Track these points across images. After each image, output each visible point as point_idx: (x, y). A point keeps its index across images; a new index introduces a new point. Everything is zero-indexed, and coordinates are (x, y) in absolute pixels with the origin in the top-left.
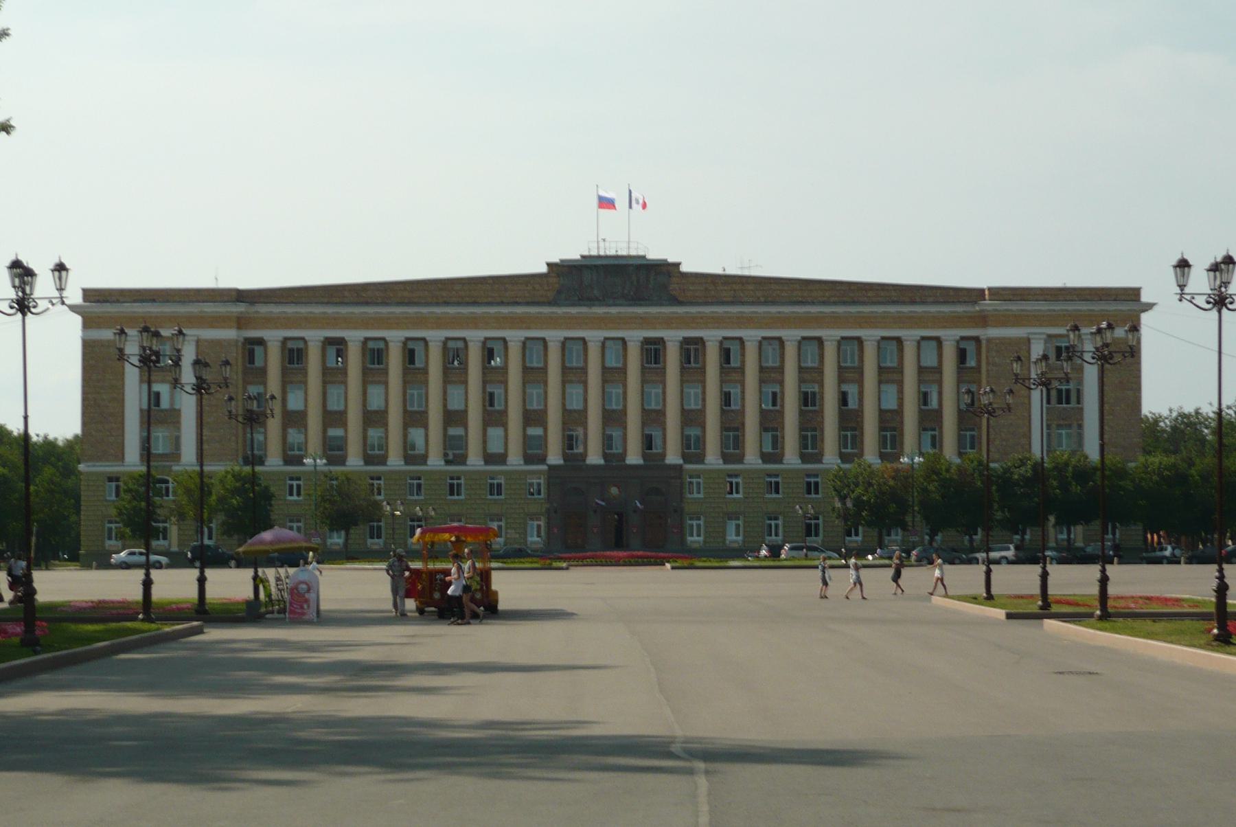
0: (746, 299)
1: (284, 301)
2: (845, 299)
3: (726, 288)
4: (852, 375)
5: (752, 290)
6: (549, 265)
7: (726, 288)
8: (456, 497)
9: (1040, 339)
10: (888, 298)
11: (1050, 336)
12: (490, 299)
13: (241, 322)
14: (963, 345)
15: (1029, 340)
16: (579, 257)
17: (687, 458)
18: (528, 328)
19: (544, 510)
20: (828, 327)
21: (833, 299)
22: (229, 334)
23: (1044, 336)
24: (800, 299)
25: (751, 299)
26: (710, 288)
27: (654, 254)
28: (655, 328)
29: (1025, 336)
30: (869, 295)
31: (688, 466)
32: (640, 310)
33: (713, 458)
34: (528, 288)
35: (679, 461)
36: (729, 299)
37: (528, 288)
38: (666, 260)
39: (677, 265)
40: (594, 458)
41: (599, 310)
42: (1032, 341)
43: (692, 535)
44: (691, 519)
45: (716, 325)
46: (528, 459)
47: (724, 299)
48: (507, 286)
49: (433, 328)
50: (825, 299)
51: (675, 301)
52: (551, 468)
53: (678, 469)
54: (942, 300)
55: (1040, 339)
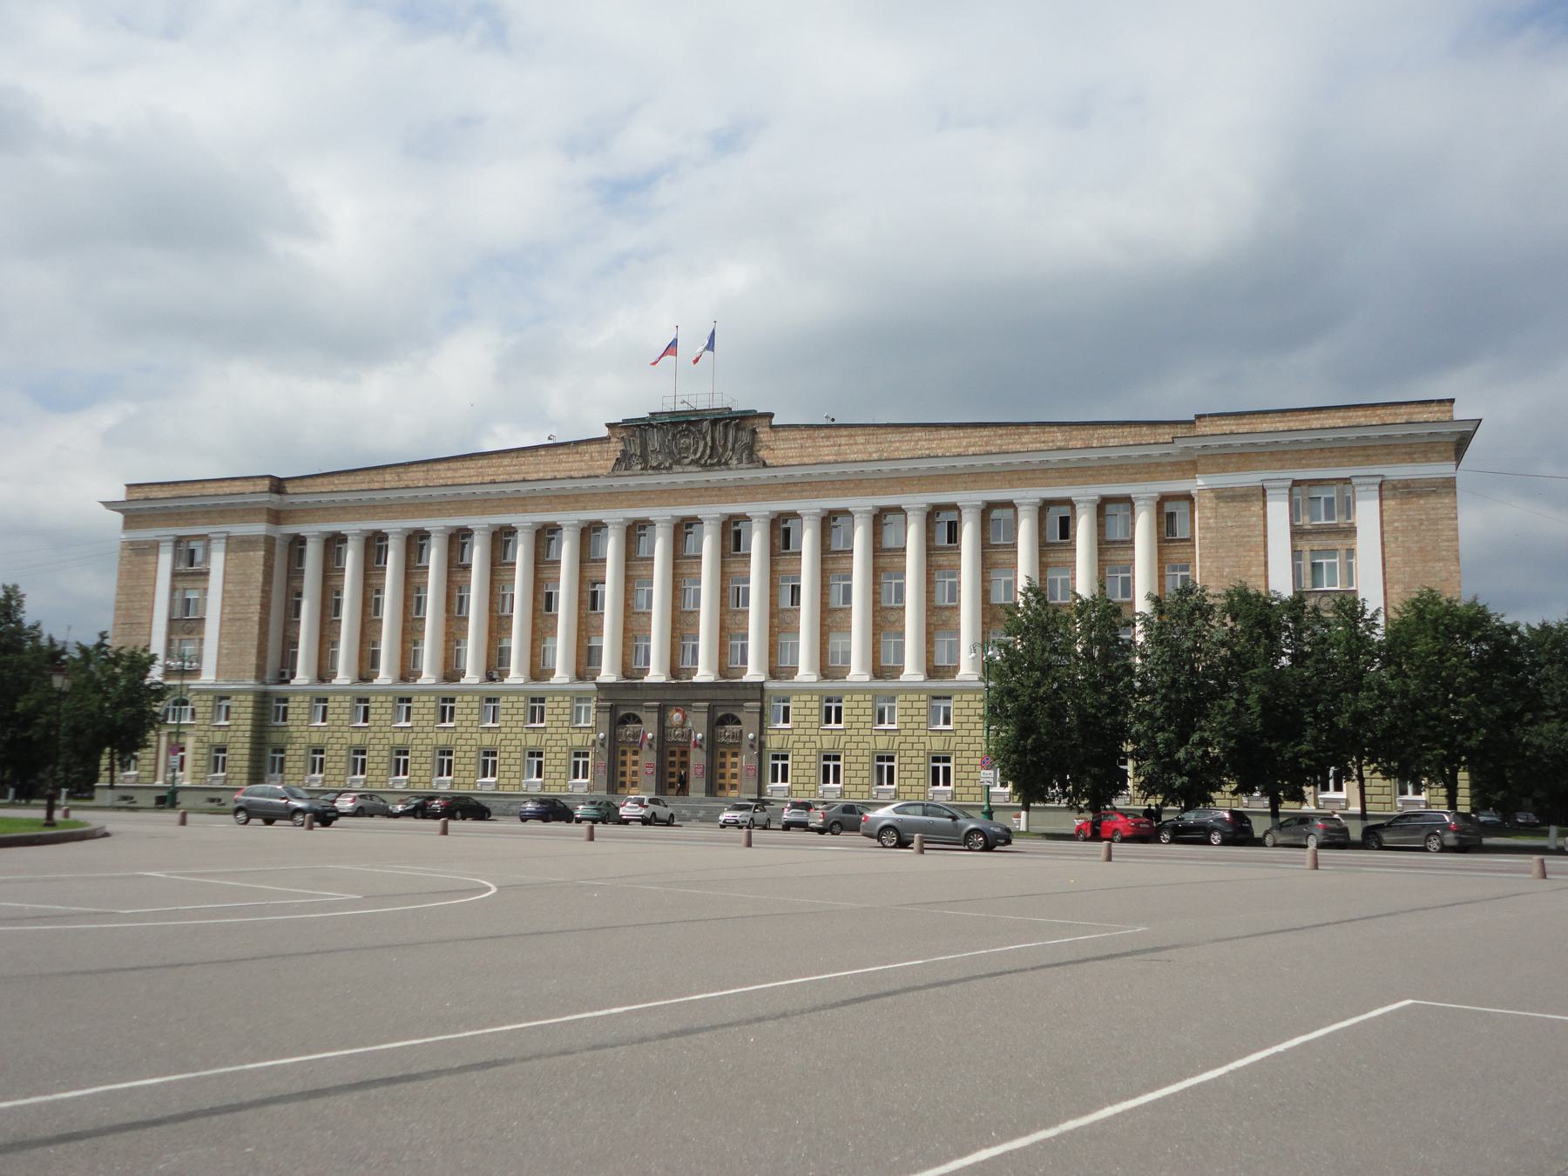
0: (853, 457)
1: (323, 490)
2: (988, 448)
3: (828, 443)
4: (1005, 557)
5: (862, 444)
6: (610, 426)
7: (828, 443)
8: (447, 724)
9: (1284, 487)
10: (1050, 444)
11: (1296, 483)
12: (541, 475)
13: (276, 517)
14: (1169, 507)
15: (1264, 490)
16: (648, 415)
17: (774, 673)
18: (585, 508)
19: (590, 743)
20: (965, 489)
21: (971, 450)
22: (259, 528)
23: (1290, 483)
24: (927, 452)
25: (860, 457)
26: (807, 445)
27: (739, 406)
28: (735, 501)
29: (1261, 484)
30: (1023, 440)
31: (772, 685)
32: (715, 476)
33: (806, 673)
34: (585, 458)
35: (762, 679)
36: (830, 458)
37: (585, 458)
38: (755, 411)
39: (771, 415)
40: (656, 673)
41: (664, 479)
42: (1268, 492)
43: (775, 780)
44: (776, 757)
45: (815, 493)
46: (580, 676)
47: (827, 458)
48: (561, 457)
49: (477, 514)
50: (961, 450)
51: (765, 465)
52: (602, 687)
53: (760, 687)
54: (1131, 443)
55: (1284, 487)
